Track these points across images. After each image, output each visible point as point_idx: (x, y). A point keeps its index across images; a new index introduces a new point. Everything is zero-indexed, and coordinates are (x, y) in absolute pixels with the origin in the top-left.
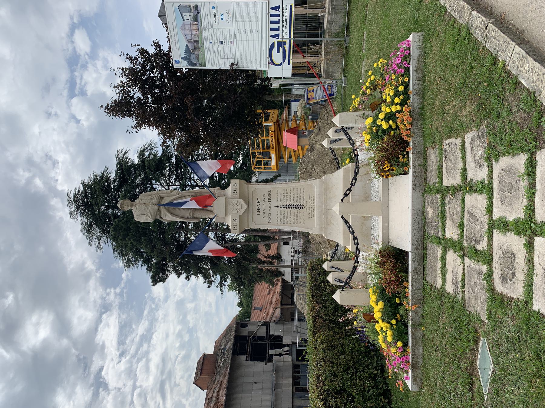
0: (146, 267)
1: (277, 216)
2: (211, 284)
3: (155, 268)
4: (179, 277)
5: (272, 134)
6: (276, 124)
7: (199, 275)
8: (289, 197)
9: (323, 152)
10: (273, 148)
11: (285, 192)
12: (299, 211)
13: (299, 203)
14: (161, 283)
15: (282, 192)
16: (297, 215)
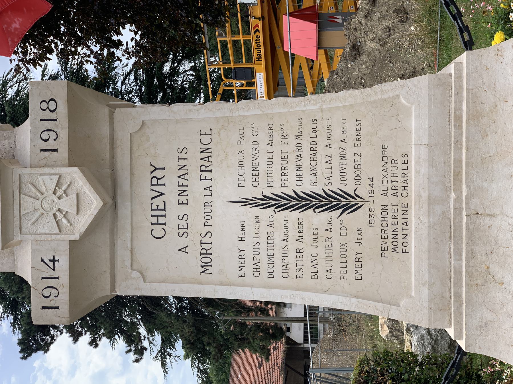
0: (11, 319)
1: (242, 245)
2: (142, 354)
4: (76, 340)
5: (257, 26)
7: (117, 337)
8: (292, 158)
9: (384, 59)
10: (259, 59)
11: (277, 138)
12: (336, 224)
13: (335, 186)
14: (40, 353)
15: (263, 138)
16: (328, 239)
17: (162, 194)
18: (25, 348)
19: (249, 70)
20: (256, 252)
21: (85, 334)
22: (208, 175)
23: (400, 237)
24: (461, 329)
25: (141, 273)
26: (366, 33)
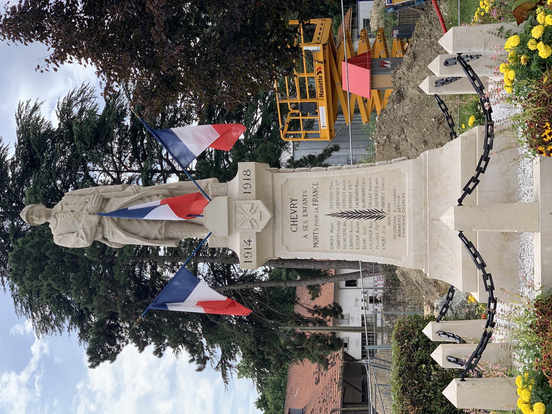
0: (78, 330)
1: (332, 234)
2: (205, 363)
3: (96, 334)
4: (141, 349)
5: (320, 68)
6: (327, 47)
7: (180, 347)
8: (354, 195)
9: (422, 103)
10: (321, 96)
12: (374, 224)
13: (373, 208)
14: (107, 362)
15: (341, 186)
16: (370, 231)
17: (296, 212)
18: (93, 357)
19: (313, 105)
20: (338, 237)
21: (150, 344)
22: (317, 203)
23: (402, 230)
24: (427, 269)
25: (287, 247)
26: (408, 82)
